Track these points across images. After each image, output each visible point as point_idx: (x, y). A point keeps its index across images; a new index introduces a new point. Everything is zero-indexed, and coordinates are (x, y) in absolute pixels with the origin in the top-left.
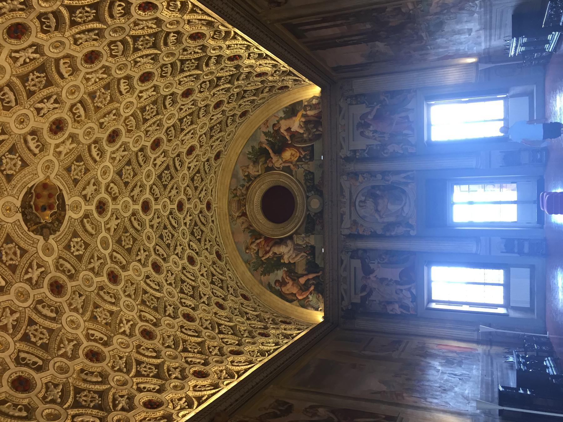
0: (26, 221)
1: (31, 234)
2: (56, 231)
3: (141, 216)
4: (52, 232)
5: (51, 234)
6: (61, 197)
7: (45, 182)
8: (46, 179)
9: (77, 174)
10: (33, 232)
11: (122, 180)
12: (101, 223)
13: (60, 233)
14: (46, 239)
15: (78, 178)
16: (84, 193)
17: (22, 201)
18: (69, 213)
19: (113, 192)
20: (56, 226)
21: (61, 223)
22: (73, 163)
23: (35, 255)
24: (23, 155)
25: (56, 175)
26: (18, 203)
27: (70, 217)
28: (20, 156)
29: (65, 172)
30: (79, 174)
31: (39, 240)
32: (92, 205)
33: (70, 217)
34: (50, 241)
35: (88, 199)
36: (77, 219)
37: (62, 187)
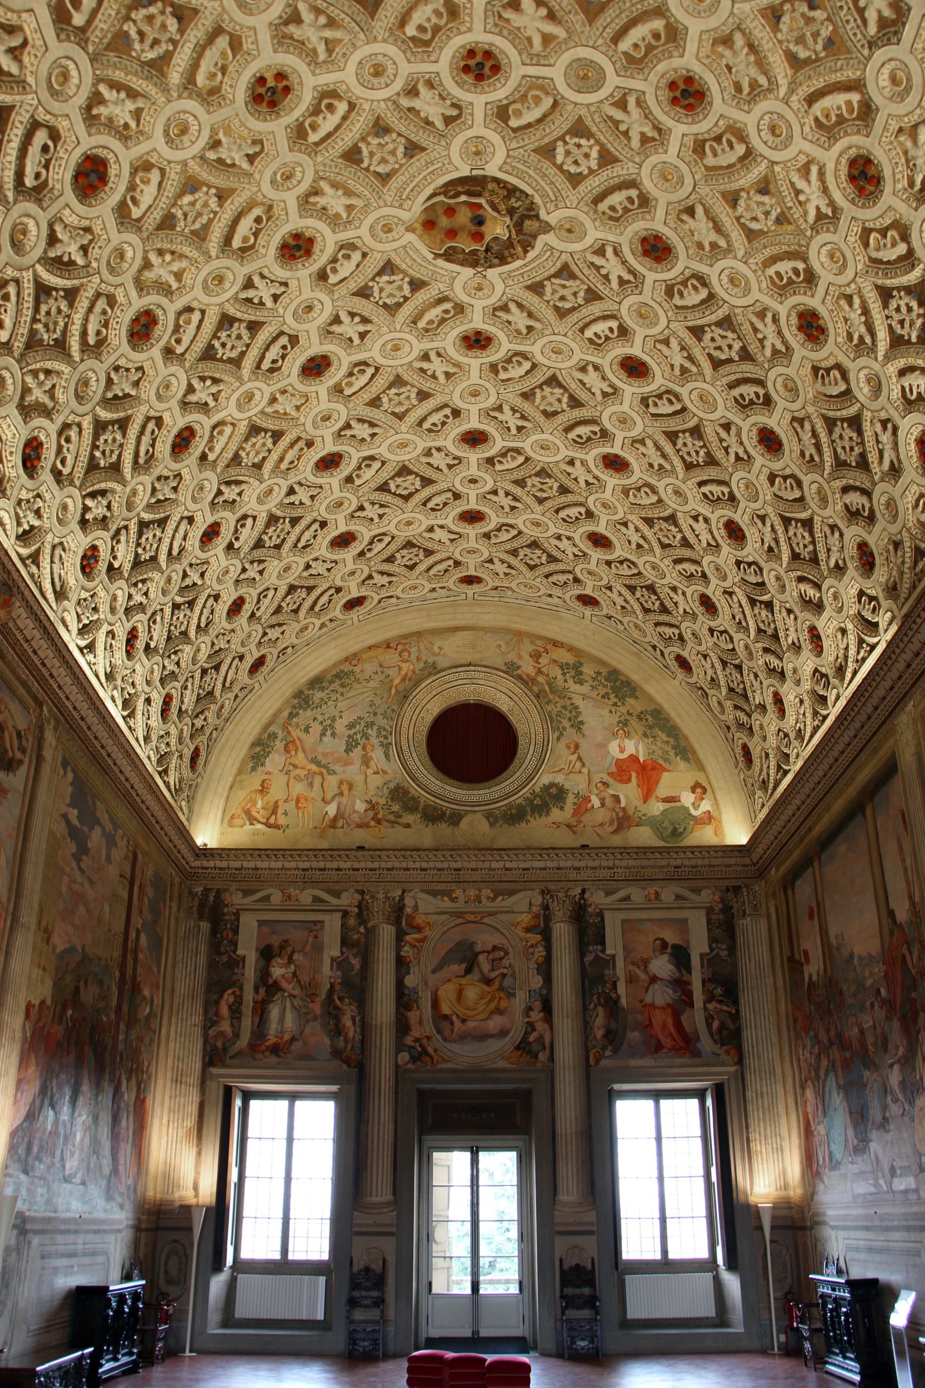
0: (503, 261)
1: (531, 255)
2: (532, 203)
4: (533, 213)
5: (537, 216)
6: (453, 187)
9: (393, 153)
10: (526, 252)
12: (524, 77)
13: (536, 196)
14: (547, 228)
15: (401, 149)
16: (439, 124)
17: (462, 265)
18: (492, 169)
19: (434, 20)
20: (519, 203)
21: (512, 191)
22: (367, 169)
23: (576, 257)
24: (370, 276)
25: (401, 206)
26: (467, 272)
27: (500, 169)
28: (373, 279)
29: (394, 184)
30: (391, 147)
31: (546, 244)
32: (471, 104)
33: (500, 169)
35: (455, 112)
36: (508, 151)
37: (429, 191)
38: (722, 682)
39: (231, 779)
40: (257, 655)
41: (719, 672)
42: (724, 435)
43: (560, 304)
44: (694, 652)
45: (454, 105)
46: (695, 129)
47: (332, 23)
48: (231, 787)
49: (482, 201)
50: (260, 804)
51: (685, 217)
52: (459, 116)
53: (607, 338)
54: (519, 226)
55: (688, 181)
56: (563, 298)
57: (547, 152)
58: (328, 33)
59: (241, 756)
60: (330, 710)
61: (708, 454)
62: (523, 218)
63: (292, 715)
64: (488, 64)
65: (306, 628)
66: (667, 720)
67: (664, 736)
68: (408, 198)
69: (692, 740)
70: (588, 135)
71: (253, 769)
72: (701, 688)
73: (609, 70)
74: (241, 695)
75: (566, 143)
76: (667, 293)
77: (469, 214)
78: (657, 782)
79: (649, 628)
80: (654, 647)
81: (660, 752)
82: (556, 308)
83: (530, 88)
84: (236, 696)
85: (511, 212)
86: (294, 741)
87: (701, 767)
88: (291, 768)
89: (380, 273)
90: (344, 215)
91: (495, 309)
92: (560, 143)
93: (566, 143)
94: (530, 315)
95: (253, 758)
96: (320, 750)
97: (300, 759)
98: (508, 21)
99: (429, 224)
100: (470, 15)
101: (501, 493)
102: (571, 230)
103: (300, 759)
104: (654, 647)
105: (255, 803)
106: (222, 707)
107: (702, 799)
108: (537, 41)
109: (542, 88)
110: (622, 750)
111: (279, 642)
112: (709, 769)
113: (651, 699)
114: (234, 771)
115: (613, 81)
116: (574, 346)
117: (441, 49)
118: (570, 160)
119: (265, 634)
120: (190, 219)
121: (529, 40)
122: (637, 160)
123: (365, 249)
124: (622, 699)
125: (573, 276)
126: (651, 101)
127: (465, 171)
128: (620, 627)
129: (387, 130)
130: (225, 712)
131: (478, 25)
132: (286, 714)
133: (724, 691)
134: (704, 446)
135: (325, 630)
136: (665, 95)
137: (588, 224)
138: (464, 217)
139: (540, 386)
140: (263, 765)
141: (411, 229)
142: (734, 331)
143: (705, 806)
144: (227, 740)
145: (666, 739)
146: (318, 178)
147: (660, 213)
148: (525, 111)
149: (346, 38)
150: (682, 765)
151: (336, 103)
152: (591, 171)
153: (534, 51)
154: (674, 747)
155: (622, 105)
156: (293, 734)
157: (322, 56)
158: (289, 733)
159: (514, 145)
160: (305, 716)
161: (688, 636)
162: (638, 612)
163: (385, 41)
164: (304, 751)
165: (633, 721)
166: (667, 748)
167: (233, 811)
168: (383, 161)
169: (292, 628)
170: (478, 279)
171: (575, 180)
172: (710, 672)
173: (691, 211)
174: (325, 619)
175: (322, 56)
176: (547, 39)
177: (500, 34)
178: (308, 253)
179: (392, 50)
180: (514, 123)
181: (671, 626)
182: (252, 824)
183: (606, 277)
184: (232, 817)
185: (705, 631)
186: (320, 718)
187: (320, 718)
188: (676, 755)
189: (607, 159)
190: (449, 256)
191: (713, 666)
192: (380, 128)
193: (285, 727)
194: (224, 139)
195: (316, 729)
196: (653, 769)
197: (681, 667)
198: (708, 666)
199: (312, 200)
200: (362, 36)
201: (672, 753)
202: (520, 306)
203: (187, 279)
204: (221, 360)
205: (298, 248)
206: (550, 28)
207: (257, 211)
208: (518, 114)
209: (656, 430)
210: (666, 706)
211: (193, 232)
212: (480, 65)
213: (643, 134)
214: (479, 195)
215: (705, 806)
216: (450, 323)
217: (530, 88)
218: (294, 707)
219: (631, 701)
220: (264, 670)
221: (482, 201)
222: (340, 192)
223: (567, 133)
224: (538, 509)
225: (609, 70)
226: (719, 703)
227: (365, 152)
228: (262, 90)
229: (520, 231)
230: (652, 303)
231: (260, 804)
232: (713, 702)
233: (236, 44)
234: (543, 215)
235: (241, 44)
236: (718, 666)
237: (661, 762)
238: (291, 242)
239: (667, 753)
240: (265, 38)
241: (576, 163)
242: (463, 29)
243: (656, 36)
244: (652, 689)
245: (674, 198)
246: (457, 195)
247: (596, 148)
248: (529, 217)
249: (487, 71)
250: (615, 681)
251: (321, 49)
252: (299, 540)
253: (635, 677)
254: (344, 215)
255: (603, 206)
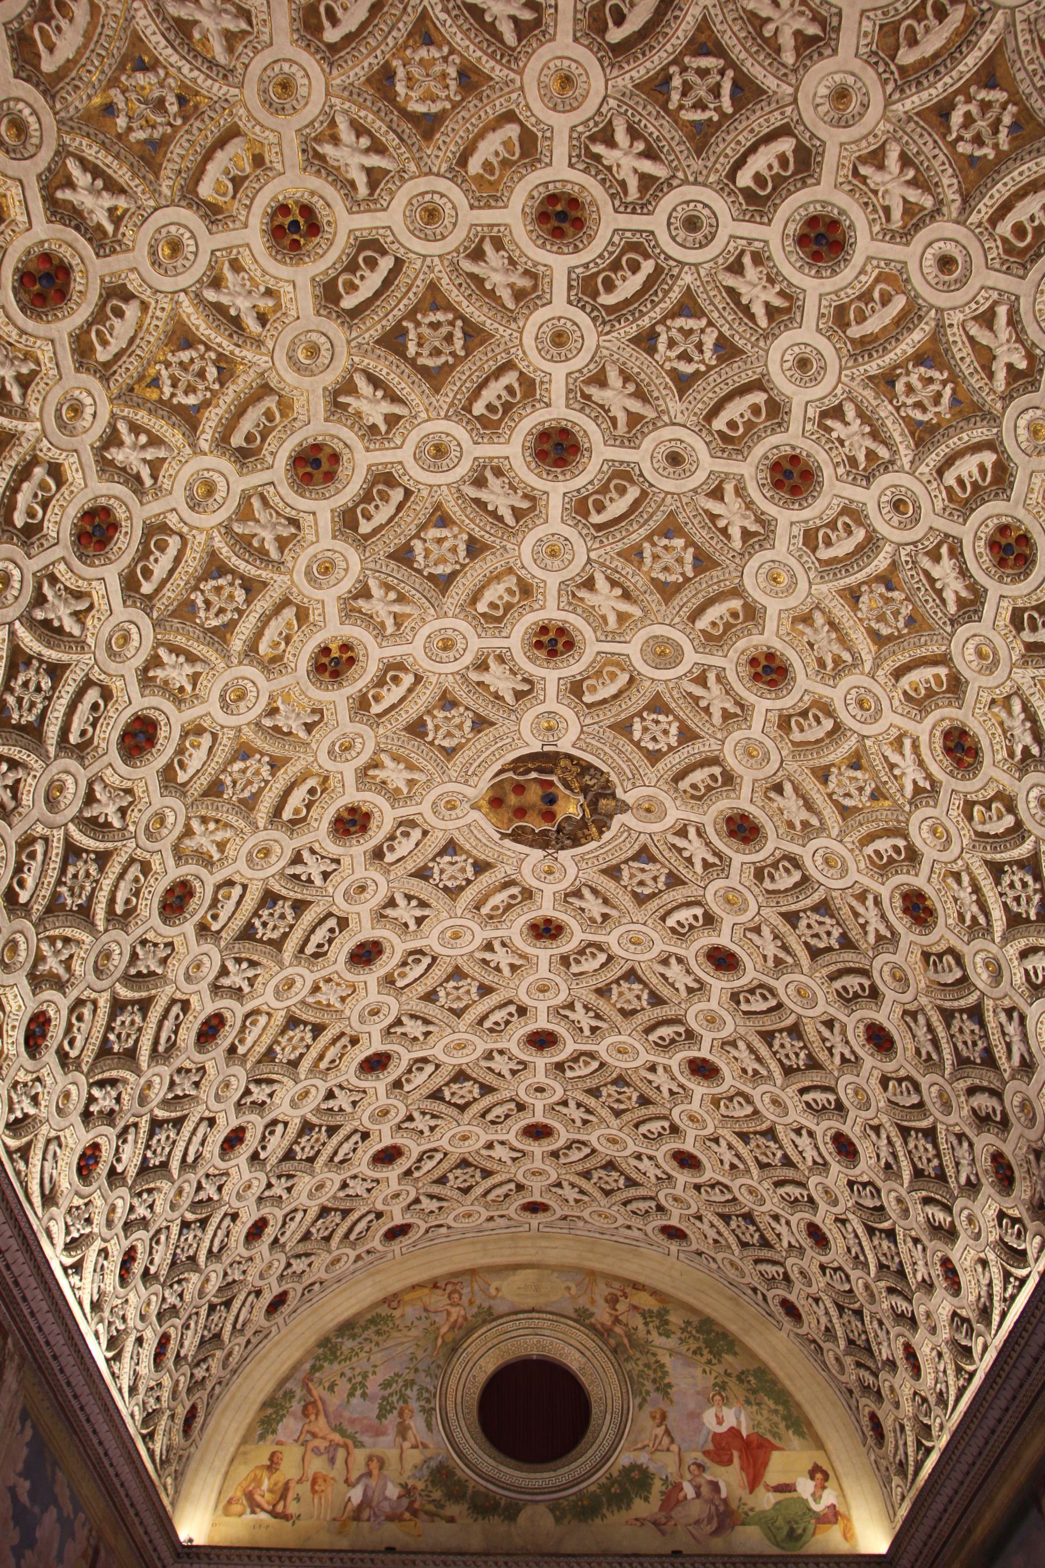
0: (576, 842)
1: (607, 836)
3: (591, 482)
5: (613, 795)
6: (521, 764)
7: (486, 808)
8: (479, 809)
9: (460, 727)
10: (601, 832)
11: (463, 566)
14: (623, 807)
15: (468, 724)
16: (509, 698)
18: (565, 746)
19: (507, 598)
21: (587, 768)
25: (466, 782)
26: (537, 854)
28: (433, 859)
29: (460, 759)
30: (457, 721)
34: (630, 802)
37: (497, 767)
38: (840, 1333)
39: (232, 1449)
40: (277, 1290)
41: (835, 1320)
42: (826, 1033)
43: (639, 890)
44: (803, 1295)
45: (525, 680)
46: (779, 704)
47: (401, 599)
48: (232, 1461)
49: (554, 778)
50: (265, 1485)
51: (772, 795)
52: (530, 691)
53: (691, 927)
54: (593, 805)
55: (775, 758)
56: (641, 883)
57: (624, 728)
58: (397, 608)
59: (248, 1420)
60: (361, 1363)
61: (810, 1056)
62: (598, 796)
63: (314, 1369)
64: (562, 641)
65: (338, 1260)
66: (775, 1381)
67: (771, 1403)
68: (474, 774)
69: (807, 1407)
70: (667, 711)
71: (262, 1437)
72: (814, 1341)
73: (687, 646)
74: (254, 1341)
75: (643, 719)
76: (756, 876)
77: (540, 792)
78: (765, 1464)
79: (748, 1266)
80: (755, 1290)
81: (766, 1424)
82: (635, 894)
83: (605, 665)
84: (248, 1342)
85: (585, 790)
86: (314, 1403)
87: (820, 1445)
88: (309, 1437)
89: (441, 853)
90: (405, 790)
91: (566, 895)
92: (637, 719)
93: (643, 719)
94: (606, 902)
95: (262, 1422)
96: (346, 1414)
97: (321, 1425)
98: (582, 599)
99: (496, 802)
100: (544, 594)
101: (572, 1104)
102: (650, 810)
103: (321, 1425)
104: (755, 1290)
105: (259, 1484)
106: (230, 1354)
107: (824, 1488)
108: (612, 619)
109: (618, 664)
110: (720, 1421)
111: (305, 1277)
112: (830, 1446)
113: (753, 1356)
114: (237, 1439)
115: (691, 657)
116: (654, 936)
117: (513, 625)
118: (647, 737)
119: (289, 1265)
120: (239, 787)
121: (604, 618)
122: (719, 736)
123: (426, 827)
124: (717, 1355)
125: (652, 859)
126: (732, 677)
127: (535, 747)
128: (713, 1266)
129: (454, 704)
130: (234, 1360)
131: (552, 602)
132: (307, 1366)
133: (842, 1343)
134: (805, 1047)
135: (360, 1263)
136: (746, 671)
137: (668, 803)
138: (534, 795)
139: (617, 982)
140: (274, 1432)
141: (475, 807)
142: (832, 916)
143: (829, 1497)
144: (233, 1397)
145: (773, 1406)
146: (379, 750)
147: (746, 791)
148: (599, 687)
149: (416, 612)
150: (796, 1441)
151: (402, 675)
152: (671, 748)
153: (609, 629)
154: (784, 1418)
155: (701, 680)
156: (315, 1393)
157: (390, 629)
158: (309, 1391)
159: (588, 721)
160: (331, 1371)
161: (794, 1275)
162: (734, 1247)
163: (455, 616)
164: (326, 1416)
165: (732, 1383)
166: (776, 1419)
167: (230, 1494)
168: (449, 735)
169: (321, 1260)
170: (549, 862)
171: (654, 757)
172: (824, 1320)
173: (779, 789)
174: (361, 1250)
175: (390, 629)
176: (622, 617)
177: (574, 612)
178: (364, 829)
179: (463, 626)
180: (588, 698)
181: (774, 1263)
182: (253, 1512)
183: (689, 860)
184: (230, 1502)
185: (815, 1269)
186: (349, 1373)
187: (349, 1373)
188: (788, 1427)
189: (687, 735)
190: (517, 836)
191: (827, 1313)
192: (448, 702)
193: (305, 1385)
194: (282, 707)
195: (343, 1386)
196: (760, 1446)
197: (788, 1314)
198: (821, 1312)
199: (371, 772)
200: (432, 611)
201: (782, 1425)
202: (595, 892)
203: (230, 850)
204: (260, 941)
205: (353, 822)
206: (625, 607)
207: (311, 782)
208: (593, 689)
209: (749, 1030)
210: (772, 1365)
211: (240, 801)
212: (553, 642)
213: (724, 710)
214: (551, 772)
215: (829, 1497)
216: (517, 910)
217: (605, 665)
218: (318, 1358)
219: (728, 1358)
220: (285, 1309)
221: (554, 778)
222: (402, 766)
223: (645, 708)
224: (615, 1123)
225: (687, 646)
226: (837, 1359)
227: (430, 726)
228: (325, 660)
229: (594, 811)
230: (740, 888)
231: (265, 1485)
232: (830, 1358)
233: (302, 615)
234: (619, 793)
235: (307, 616)
236: (833, 1312)
237: (769, 1437)
238: (345, 815)
239: (776, 1425)
240: (333, 611)
241: (654, 739)
242: (536, 606)
243: (735, 615)
244: (753, 1342)
245: (760, 774)
246: (528, 771)
247: (676, 725)
248: (605, 796)
249: (560, 647)
250: (709, 1332)
251: (390, 622)
252: (335, 1153)
253: (733, 1328)
254: (405, 790)
255: (684, 785)
